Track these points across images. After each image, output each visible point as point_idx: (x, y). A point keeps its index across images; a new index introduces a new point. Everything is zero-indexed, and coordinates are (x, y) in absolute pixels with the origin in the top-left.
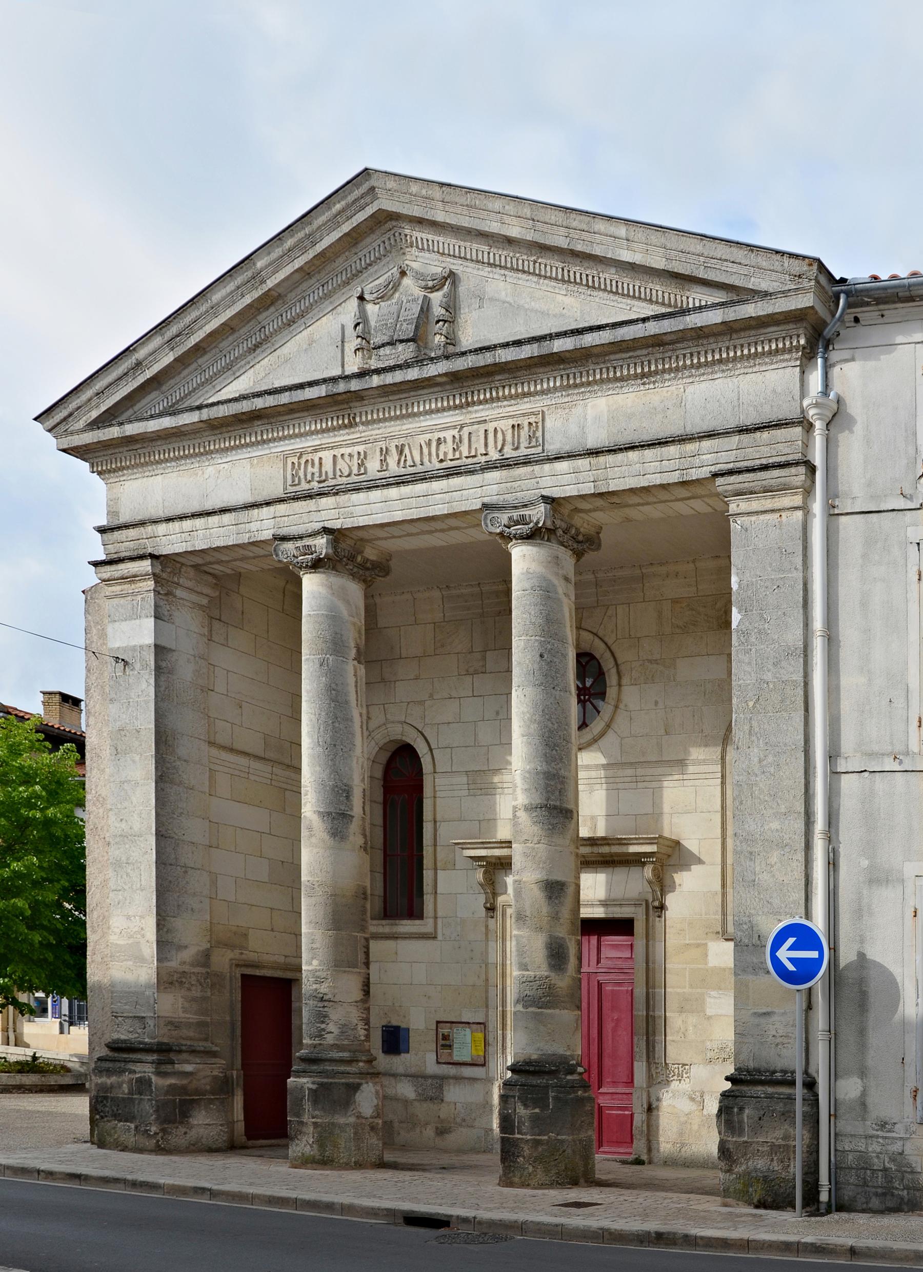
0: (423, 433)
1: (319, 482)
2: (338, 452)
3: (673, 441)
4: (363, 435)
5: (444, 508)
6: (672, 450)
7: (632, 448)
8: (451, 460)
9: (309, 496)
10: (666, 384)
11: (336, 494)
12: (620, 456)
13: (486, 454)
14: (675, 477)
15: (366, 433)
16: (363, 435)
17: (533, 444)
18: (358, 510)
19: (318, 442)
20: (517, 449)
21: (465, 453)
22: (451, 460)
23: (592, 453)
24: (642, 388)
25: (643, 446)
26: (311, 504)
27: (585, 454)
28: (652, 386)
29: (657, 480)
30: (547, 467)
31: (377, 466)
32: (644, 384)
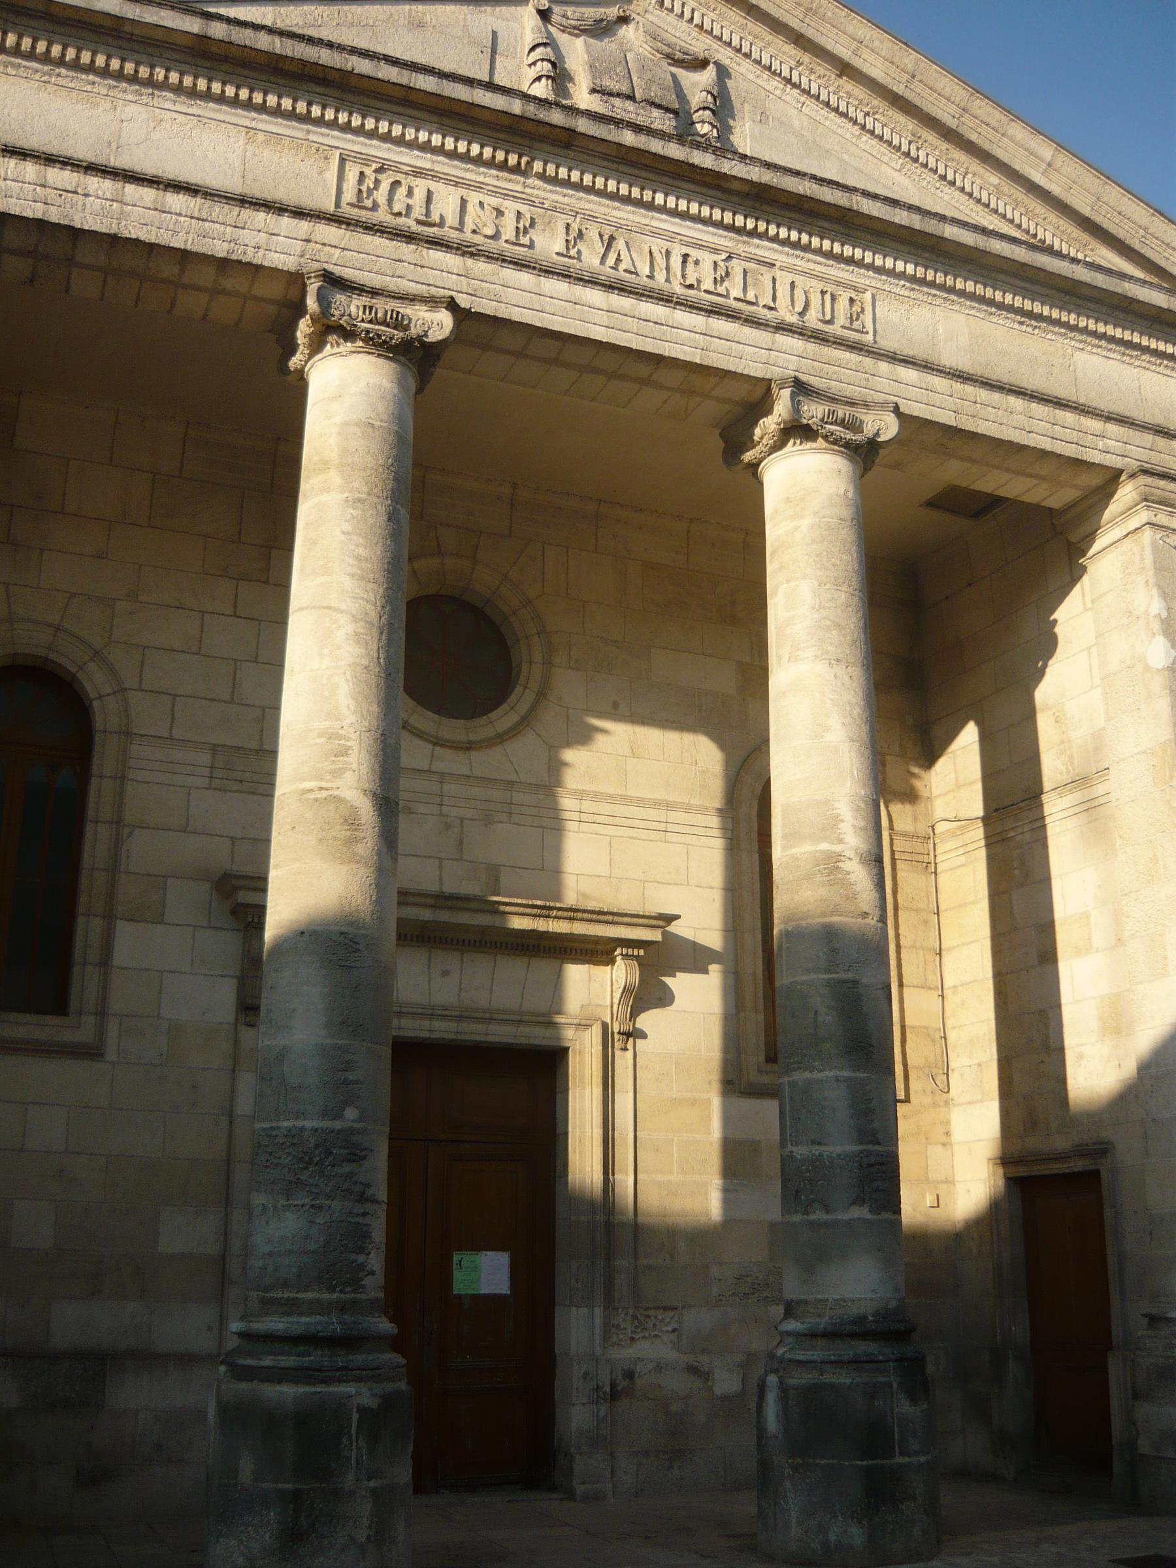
0: (655, 234)
1: (419, 222)
2: (474, 198)
3: (1076, 408)
4: (528, 190)
5: (694, 354)
6: (1069, 417)
7: (1019, 392)
8: (706, 291)
9: (409, 238)
10: (1049, 336)
11: (472, 254)
12: (996, 396)
13: (771, 308)
14: (1070, 451)
15: (535, 192)
16: (528, 190)
17: (856, 325)
18: (511, 295)
19: (428, 165)
20: (830, 322)
21: (736, 292)
22: (706, 291)
23: (959, 377)
24: (1016, 326)
25: (1032, 397)
26: (407, 250)
27: (949, 373)
28: (1029, 329)
29: (1047, 444)
30: (884, 366)
31: (559, 246)
32: (1021, 323)
